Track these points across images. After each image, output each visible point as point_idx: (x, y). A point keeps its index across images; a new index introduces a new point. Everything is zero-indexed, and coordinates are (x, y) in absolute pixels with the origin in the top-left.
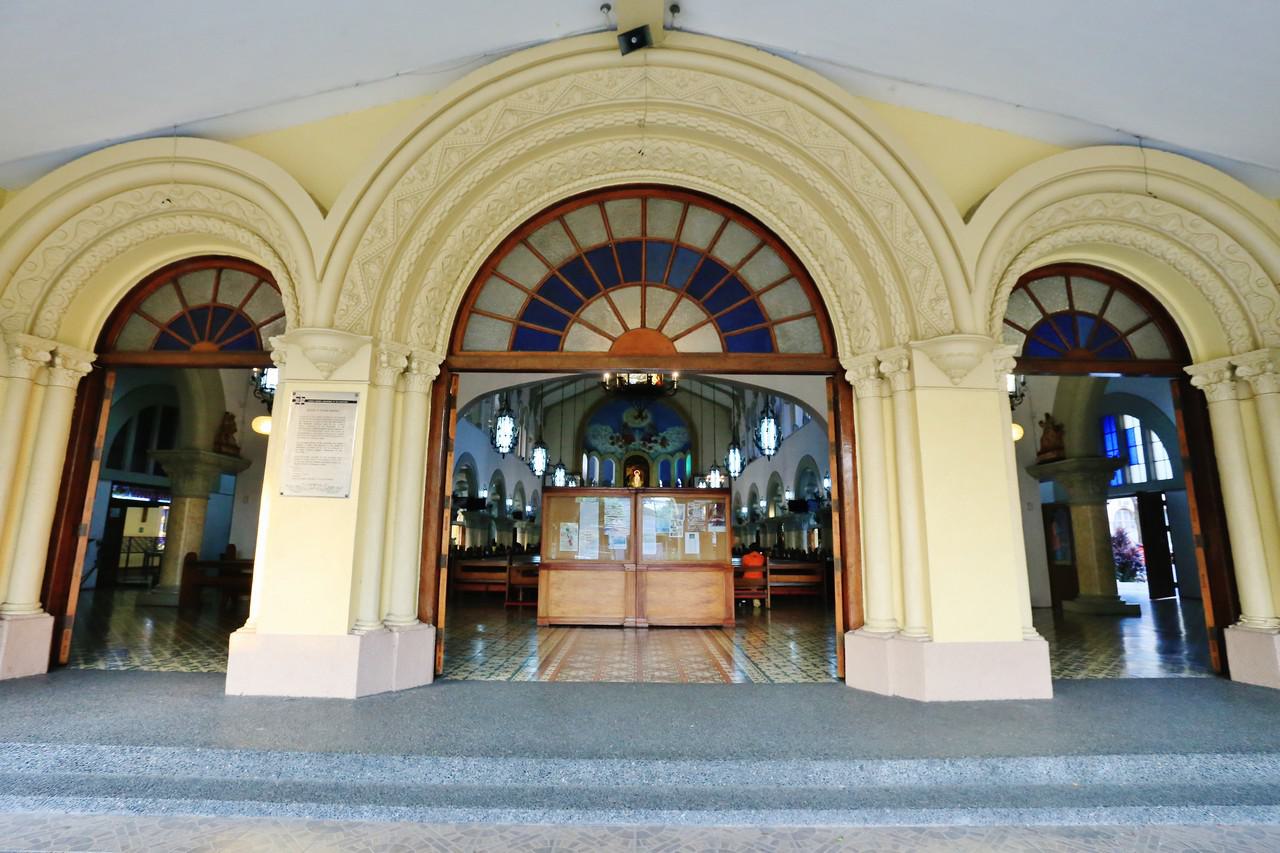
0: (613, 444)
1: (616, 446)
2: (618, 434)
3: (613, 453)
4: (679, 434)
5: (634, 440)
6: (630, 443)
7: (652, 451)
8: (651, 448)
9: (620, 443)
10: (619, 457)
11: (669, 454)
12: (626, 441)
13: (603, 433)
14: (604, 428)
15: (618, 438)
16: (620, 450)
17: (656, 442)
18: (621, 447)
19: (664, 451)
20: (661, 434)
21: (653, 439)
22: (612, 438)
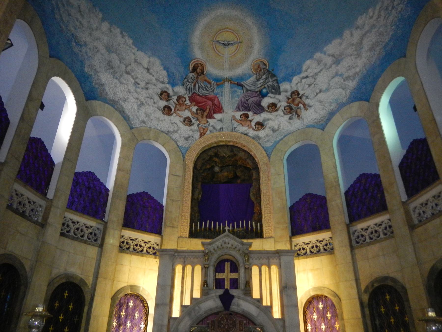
0: (167, 110)
1: (175, 118)
2: (181, 90)
3: (168, 133)
4: (337, 61)
5: (219, 109)
6: (210, 116)
7: (262, 133)
8: (260, 125)
9: (187, 114)
10: (181, 142)
11: (308, 126)
12: (202, 109)
13: (141, 73)
14: (144, 58)
15: (179, 98)
16: (185, 130)
17: (273, 107)
18: (188, 121)
19: (297, 124)
20: (284, 86)
21: (266, 102)
22: (164, 95)
